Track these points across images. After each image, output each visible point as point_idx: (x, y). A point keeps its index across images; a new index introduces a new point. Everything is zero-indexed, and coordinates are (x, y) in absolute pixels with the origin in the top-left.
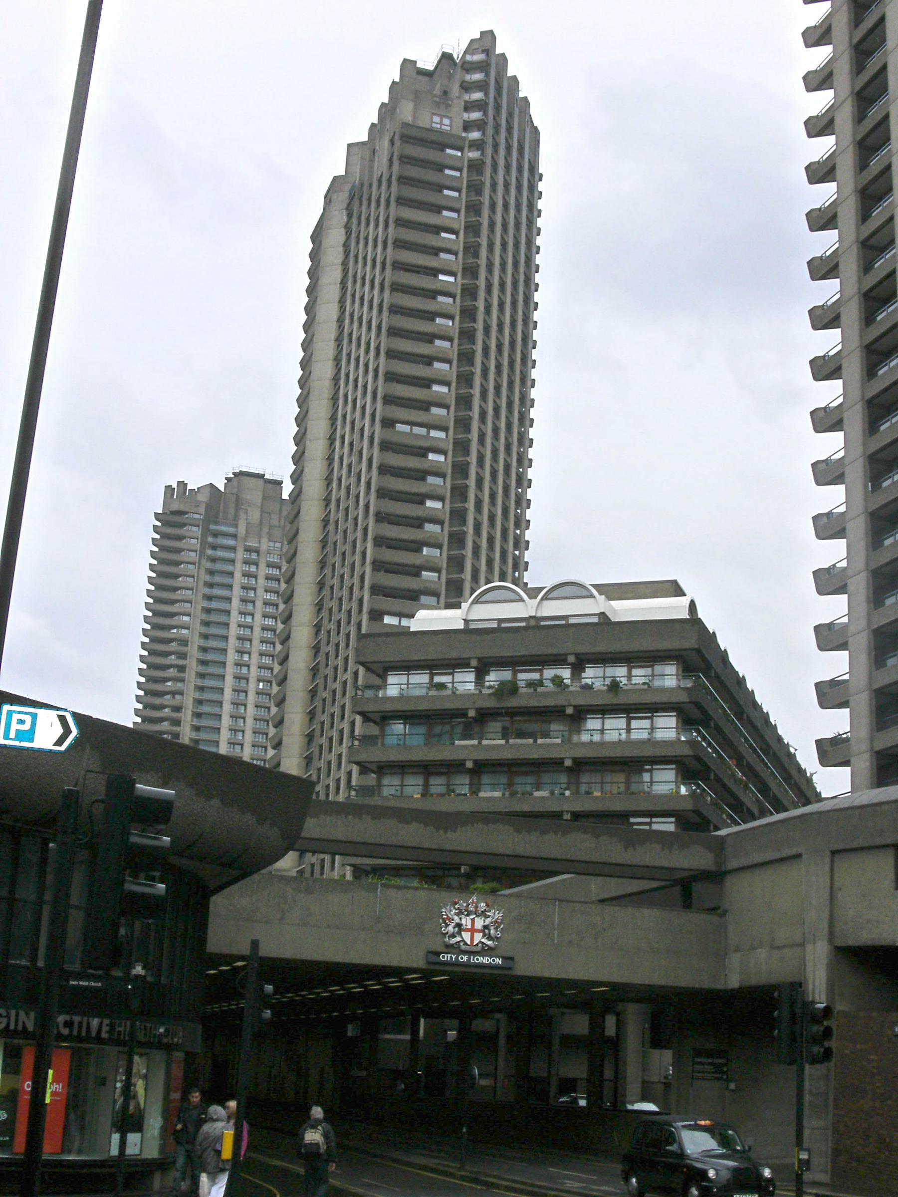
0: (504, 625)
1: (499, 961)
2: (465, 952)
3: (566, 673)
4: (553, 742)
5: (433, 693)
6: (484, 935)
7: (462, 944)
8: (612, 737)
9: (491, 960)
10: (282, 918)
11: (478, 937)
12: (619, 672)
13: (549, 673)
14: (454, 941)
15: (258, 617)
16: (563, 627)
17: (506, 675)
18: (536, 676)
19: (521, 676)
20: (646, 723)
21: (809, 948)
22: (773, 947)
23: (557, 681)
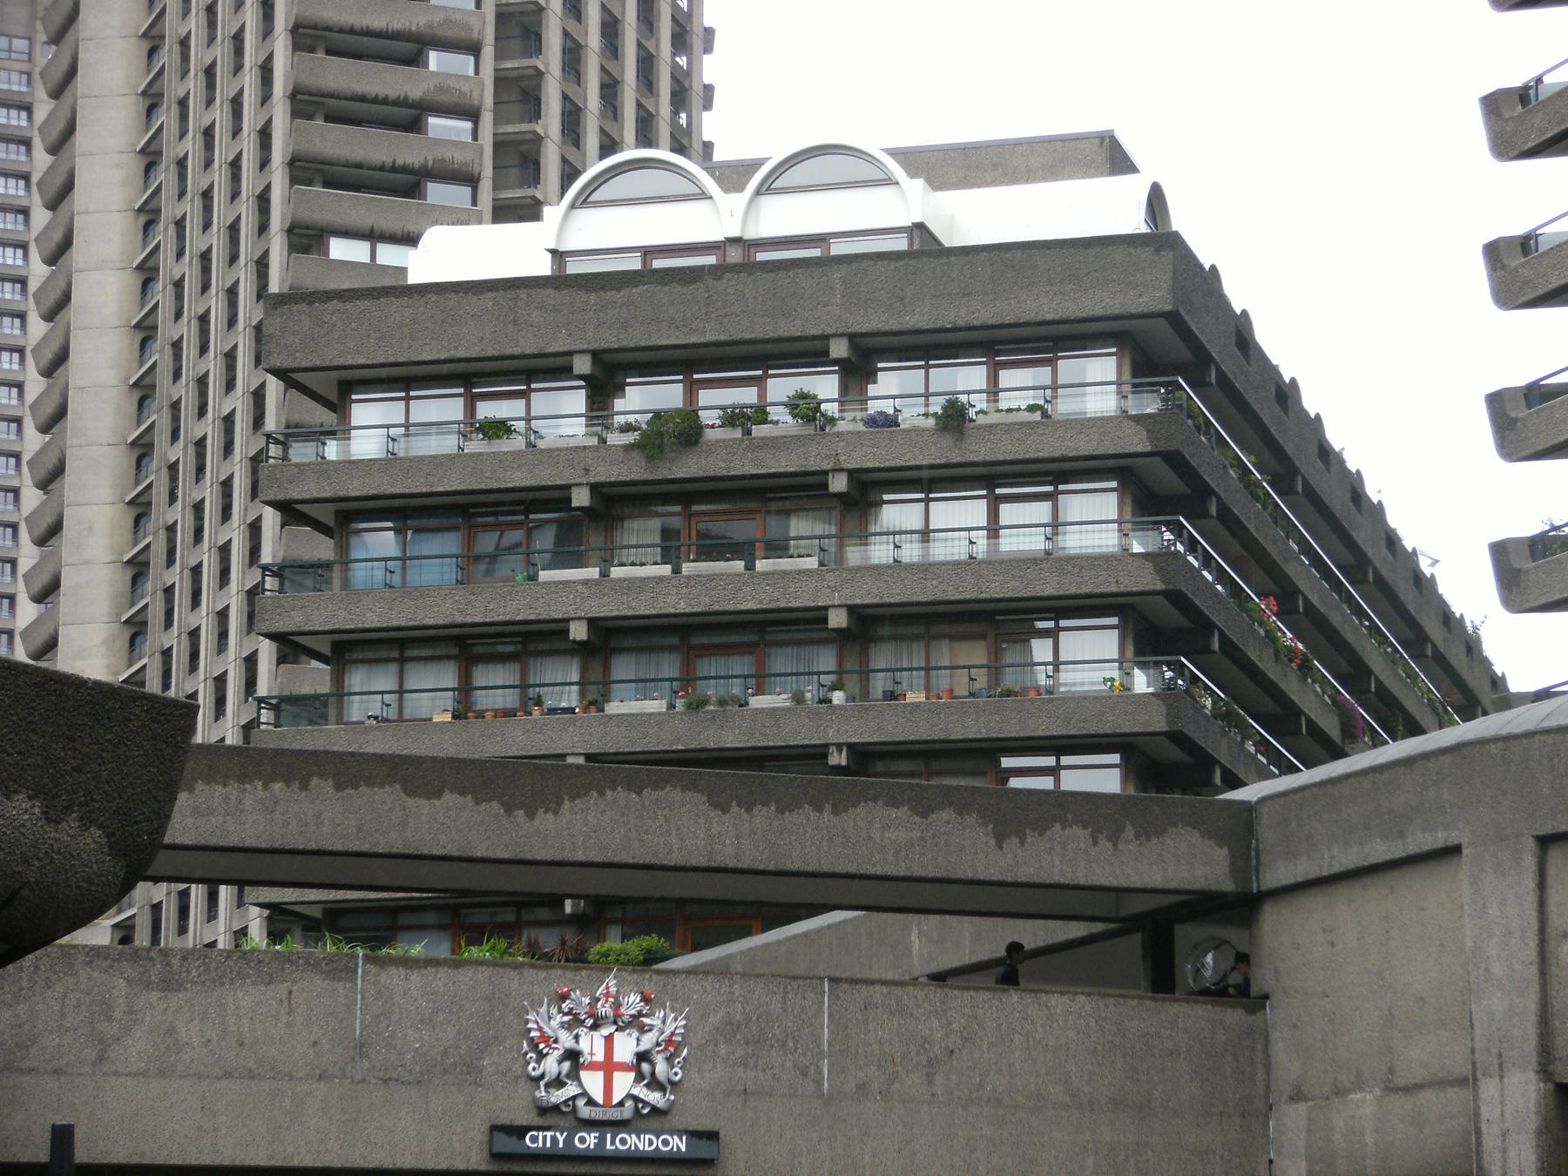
0: (658, 264)
1: (678, 1144)
2: (590, 1124)
3: (825, 386)
4: (797, 567)
5: (476, 445)
6: (640, 1077)
7: (581, 1103)
8: (947, 550)
9: (658, 1143)
10: (101, 1059)
11: (624, 1083)
12: (966, 378)
13: (781, 387)
14: (558, 1096)
16: (817, 263)
17: (664, 395)
18: (748, 395)
19: (706, 397)
20: (1039, 512)
21: (1489, 1088)
22: (1391, 1089)
23: (804, 407)
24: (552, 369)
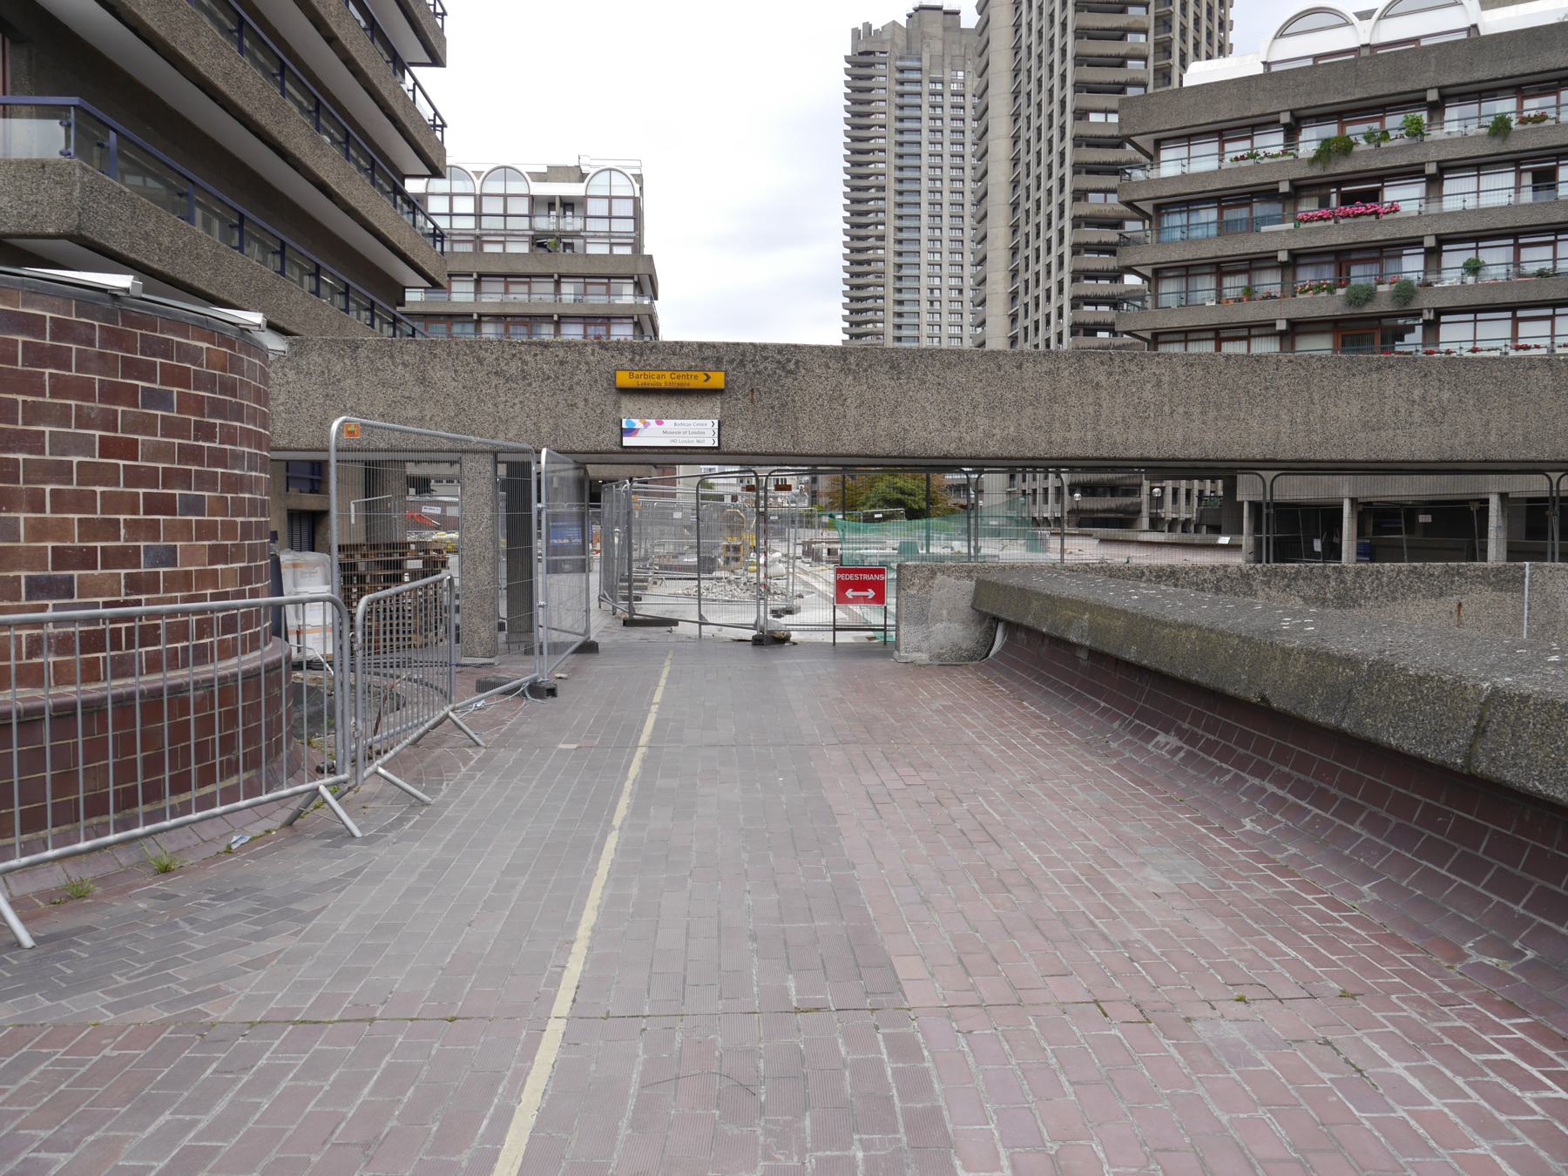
8: (1502, 199)
12: (1506, 106)
13: (1394, 121)
15: (947, 144)
16: (1411, 51)
17: (1331, 130)
19: (1350, 130)
24: (1264, 124)
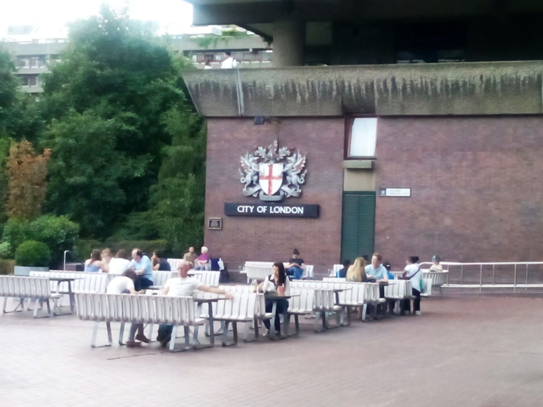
1: (300, 210)
6: (285, 182)
11: (277, 184)
14: (253, 191)
